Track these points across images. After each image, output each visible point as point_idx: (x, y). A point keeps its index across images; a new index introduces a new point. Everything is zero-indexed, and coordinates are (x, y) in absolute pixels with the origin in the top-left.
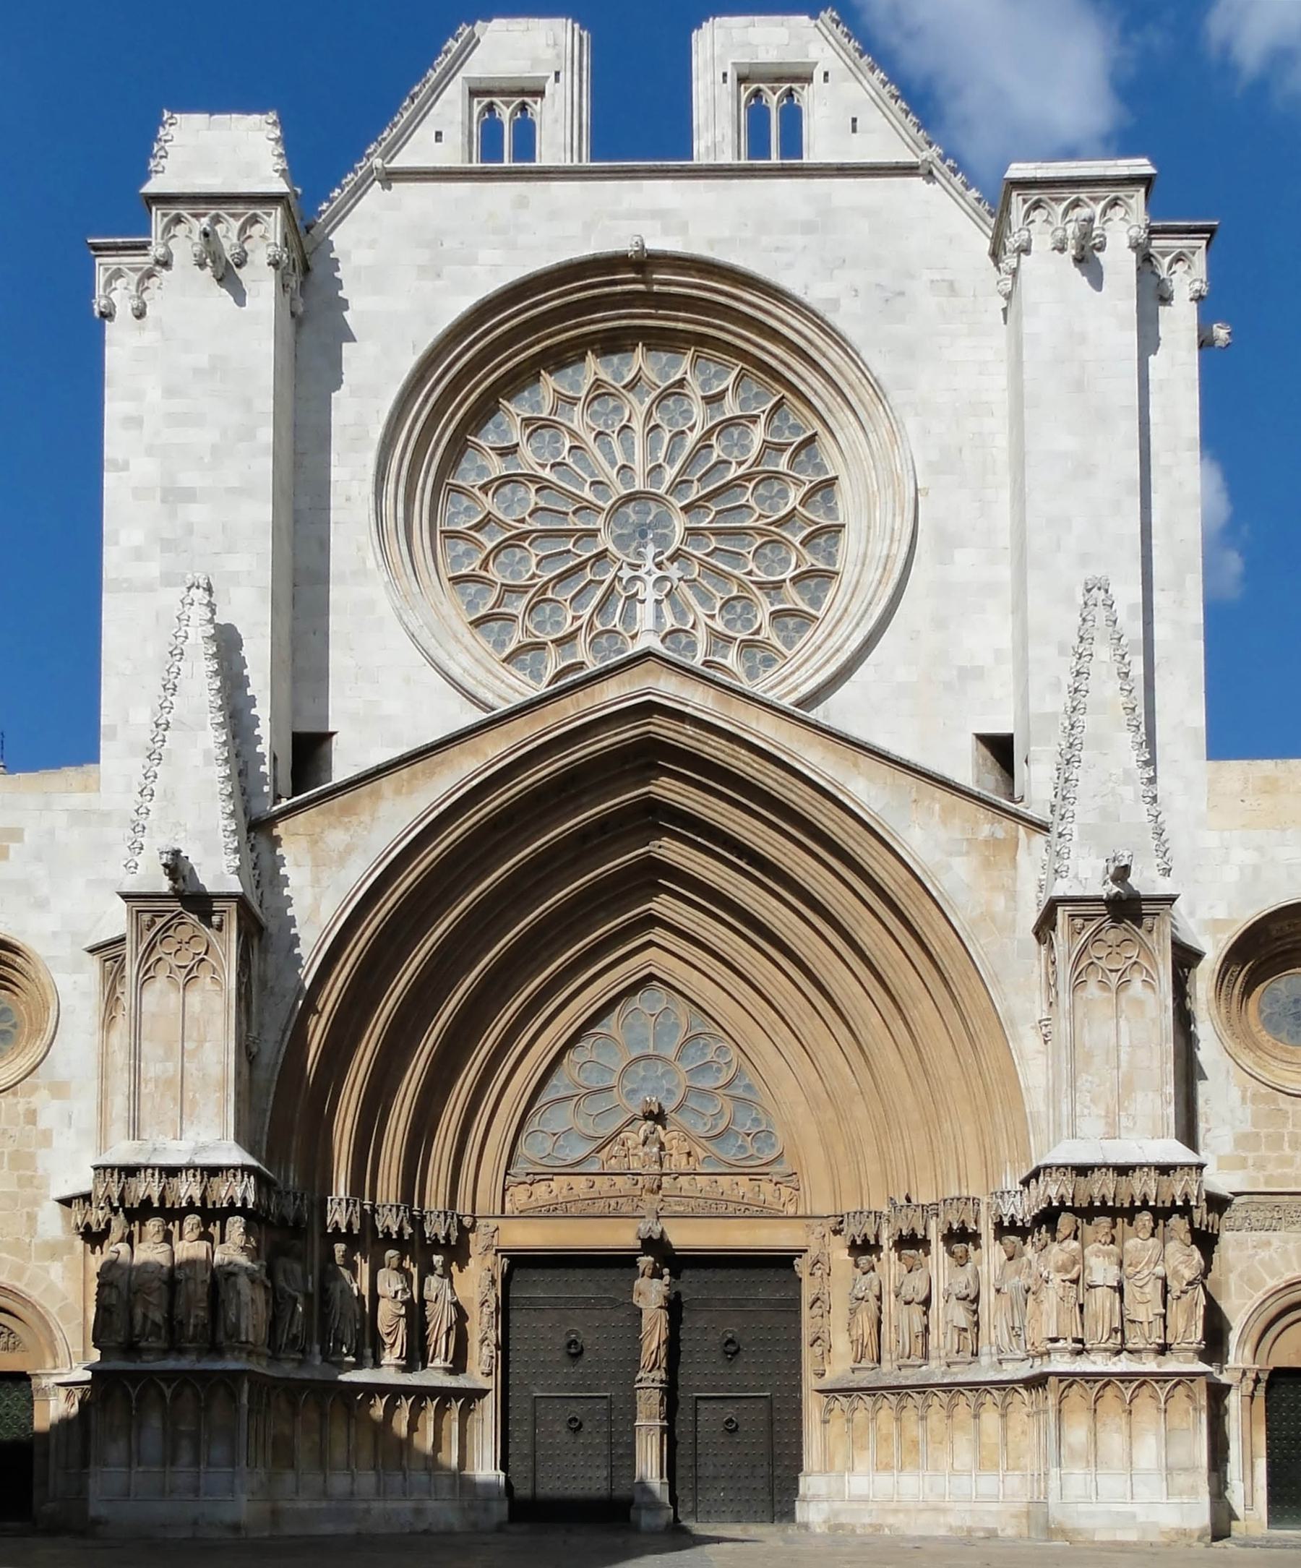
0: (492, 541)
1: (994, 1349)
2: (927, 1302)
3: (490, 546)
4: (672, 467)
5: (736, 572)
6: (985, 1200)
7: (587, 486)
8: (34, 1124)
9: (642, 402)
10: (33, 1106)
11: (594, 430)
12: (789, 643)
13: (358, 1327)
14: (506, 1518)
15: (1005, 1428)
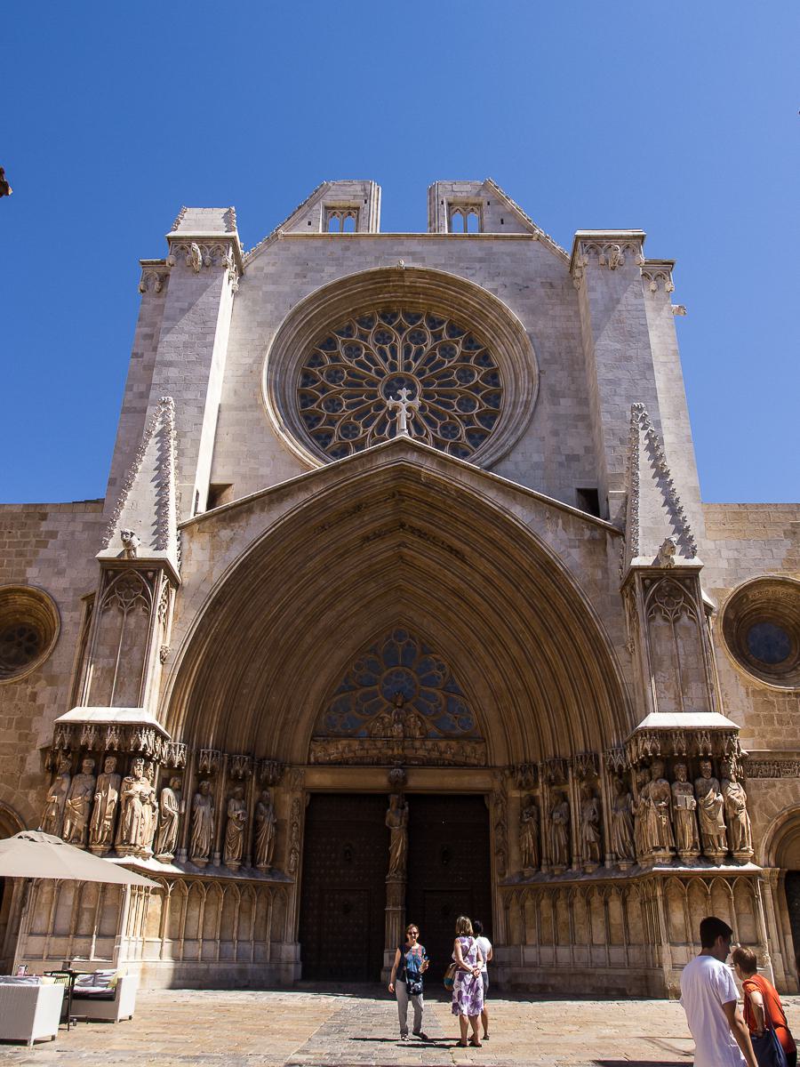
0: (323, 394)
1: (614, 856)
2: (568, 824)
3: (321, 397)
4: (415, 362)
5: (448, 411)
6: (601, 755)
7: (373, 371)
8: (34, 701)
9: (401, 334)
10: (35, 690)
11: (376, 346)
12: (476, 445)
13: (212, 837)
14: (299, 976)
15: (625, 913)
